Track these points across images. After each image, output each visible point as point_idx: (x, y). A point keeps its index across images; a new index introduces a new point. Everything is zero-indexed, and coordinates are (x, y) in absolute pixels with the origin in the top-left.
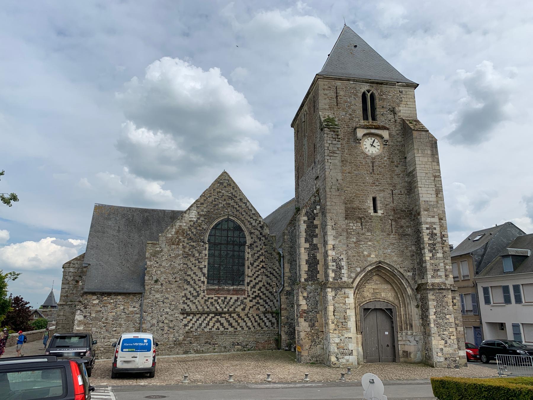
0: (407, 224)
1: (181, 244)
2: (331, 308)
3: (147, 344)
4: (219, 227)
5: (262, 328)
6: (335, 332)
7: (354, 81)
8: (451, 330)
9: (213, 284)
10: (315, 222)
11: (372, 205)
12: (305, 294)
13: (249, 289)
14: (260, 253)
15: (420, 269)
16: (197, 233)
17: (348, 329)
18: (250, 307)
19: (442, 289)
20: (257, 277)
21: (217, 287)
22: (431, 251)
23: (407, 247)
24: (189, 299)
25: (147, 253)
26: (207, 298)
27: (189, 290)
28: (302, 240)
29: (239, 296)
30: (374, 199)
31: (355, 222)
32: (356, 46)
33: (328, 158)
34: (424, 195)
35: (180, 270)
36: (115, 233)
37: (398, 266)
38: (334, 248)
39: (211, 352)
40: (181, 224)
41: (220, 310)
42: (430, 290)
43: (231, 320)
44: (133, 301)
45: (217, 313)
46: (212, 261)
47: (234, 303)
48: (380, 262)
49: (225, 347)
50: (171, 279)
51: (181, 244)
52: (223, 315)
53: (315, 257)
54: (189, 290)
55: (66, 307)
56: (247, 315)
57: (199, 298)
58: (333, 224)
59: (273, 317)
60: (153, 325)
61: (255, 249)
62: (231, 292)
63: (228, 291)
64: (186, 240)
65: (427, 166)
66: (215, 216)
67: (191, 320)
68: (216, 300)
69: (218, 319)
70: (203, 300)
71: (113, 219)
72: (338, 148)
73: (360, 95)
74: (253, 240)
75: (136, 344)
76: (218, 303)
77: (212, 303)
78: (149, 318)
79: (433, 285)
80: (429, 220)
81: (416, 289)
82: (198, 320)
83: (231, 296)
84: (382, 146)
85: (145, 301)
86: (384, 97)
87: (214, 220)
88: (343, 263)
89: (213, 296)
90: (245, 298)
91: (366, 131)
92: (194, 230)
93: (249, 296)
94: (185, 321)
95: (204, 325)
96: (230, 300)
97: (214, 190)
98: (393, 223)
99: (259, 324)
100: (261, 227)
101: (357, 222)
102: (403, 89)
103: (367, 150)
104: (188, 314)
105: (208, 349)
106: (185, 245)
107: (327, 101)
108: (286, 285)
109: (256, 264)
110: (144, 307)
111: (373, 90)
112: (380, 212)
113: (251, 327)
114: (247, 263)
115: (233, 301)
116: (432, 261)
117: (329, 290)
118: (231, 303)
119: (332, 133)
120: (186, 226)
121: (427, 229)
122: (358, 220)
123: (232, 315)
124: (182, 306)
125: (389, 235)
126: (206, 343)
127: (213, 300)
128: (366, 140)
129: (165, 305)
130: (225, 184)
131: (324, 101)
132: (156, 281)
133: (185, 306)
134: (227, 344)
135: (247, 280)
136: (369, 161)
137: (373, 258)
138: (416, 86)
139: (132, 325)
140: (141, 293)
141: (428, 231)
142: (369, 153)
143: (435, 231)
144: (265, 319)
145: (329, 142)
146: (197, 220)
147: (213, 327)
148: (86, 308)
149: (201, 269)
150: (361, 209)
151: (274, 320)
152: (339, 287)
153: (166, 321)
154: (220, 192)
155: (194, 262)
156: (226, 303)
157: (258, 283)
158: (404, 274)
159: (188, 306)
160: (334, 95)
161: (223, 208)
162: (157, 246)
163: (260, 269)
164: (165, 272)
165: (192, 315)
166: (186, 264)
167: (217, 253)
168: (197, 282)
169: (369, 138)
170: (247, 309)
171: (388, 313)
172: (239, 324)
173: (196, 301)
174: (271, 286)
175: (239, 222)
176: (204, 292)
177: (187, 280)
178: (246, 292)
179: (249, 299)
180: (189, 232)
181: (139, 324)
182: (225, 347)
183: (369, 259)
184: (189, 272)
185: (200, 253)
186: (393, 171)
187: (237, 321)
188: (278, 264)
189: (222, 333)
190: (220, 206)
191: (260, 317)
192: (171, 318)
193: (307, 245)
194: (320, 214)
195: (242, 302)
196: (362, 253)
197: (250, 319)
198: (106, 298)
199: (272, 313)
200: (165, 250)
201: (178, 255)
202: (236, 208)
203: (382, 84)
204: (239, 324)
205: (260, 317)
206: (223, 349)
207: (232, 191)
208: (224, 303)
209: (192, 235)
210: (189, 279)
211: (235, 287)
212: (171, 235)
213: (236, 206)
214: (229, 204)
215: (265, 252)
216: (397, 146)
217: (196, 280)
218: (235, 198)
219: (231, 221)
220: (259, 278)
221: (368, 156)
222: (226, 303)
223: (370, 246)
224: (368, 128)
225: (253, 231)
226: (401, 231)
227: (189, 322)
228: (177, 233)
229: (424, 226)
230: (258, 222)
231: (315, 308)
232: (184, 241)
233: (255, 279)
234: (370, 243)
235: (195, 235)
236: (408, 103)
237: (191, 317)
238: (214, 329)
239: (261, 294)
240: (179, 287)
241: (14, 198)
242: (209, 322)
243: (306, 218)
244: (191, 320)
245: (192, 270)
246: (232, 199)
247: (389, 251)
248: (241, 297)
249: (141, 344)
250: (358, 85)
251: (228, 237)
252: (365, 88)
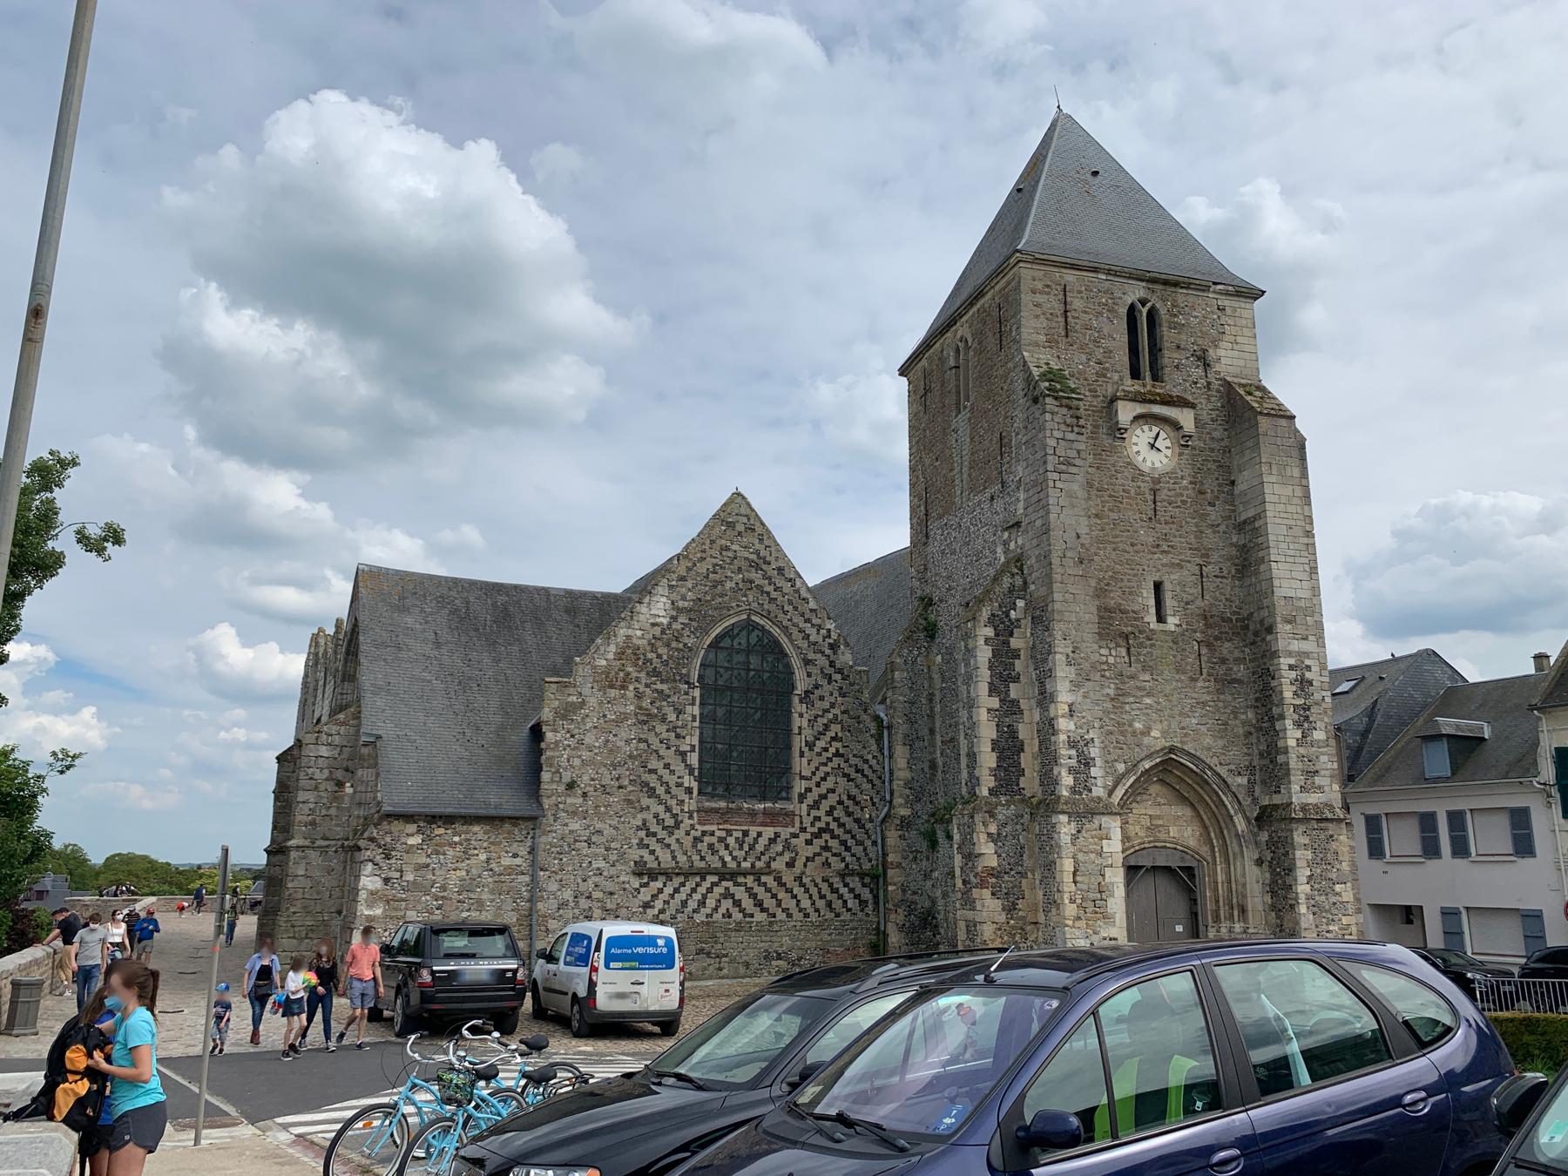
0: (1237, 654)
1: (631, 688)
2: (1068, 865)
3: (665, 950)
4: (727, 642)
5: (838, 915)
6: (1077, 924)
7: (1108, 272)
8: (1345, 920)
9: (713, 796)
10: (1015, 643)
11: (1152, 602)
12: (993, 829)
13: (804, 813)
14: (830, 716)
15: (1269, 766)
16: (671, 657)
17: (1107, 918)
18: (808, 859)
19: (1327, 820)
20: (824, 779)
21: (723, 804)
22: (1298, 725)
23: (1235, 713)
24: (654, 835)
25: (546, 710)
26: (698, 834)
27: (653, 810)
28: (983, 688)
29: (778, 829)
30: (1158, 586)
31: (1112, 645)
32: (1095, 173)
33: (1056, 476)
34: (1285, 583)
35: (630, 757)
36: (428, 649)
37: (1215, 760)
38: (1071, 713)
39: (710, 978)
40: (630, 632)
41: (732, 865)
42: (1299, 820)
43: (760, 891)
44: (511, 840)
45: (725, 875)
46: (708, 732)
47: (767, 847)
48: (1172, 750)
49: (747, 965)
50: (606, 781)
51: (631, 688)
52: (741, 880)
53: (1013, 733)
54: (653, 810)
55: (312, 854)
56: (799, 879)
57: (680, 834)
58: (1069, 650)
59: (864, 885)
60: (563, 905)
61: (818, 704)
62: (760, 818)
63: (752, 813)
64: (643, 675)
65: (1291, 509)
66: (715, 613)
67: (661, 891)
68: (721, 840)
69: (727, 889)
70: (690, 838)
71: (417, 610)
72: (1078, 452)
73: (1123, 311)
74: (812, 681)
75: (640, 950)
76: (727, 847)
77: (711, 846)
78: (553, 887)
79: (1304, 808)
80: (1296, 646)
81: (1257, 819)
82: (676, 891)
83: (760, 829)
84: (1177, 450)
85: (543, 839)
86: (1181, 319)
87: (714, 622)
88: (1094, 752)
89: (714, 828)
90: (795, 836)
91: (1140, 409)
92: (663, 651)
93: (803, 830)
94: (645, 895)
95: (692, 904)
96: (756, 840)
97: (713, 542)
98: (1204, 651)
99: (829, 904)
100: (831, 646)
101: (1118, 645)
102: (1226, 303)
103: (1140, 458)
104: (653, 875)
105: (705, 969)
106: (642, 688)
107: (1042, 323)
108: (898, 801)
109: (820, 744)
110: (541, 856)
111: (1154, 300)
112: (1172, 622)
113: (810, 910)
114: (798, 743)
115: (763, 841)
116: (1302, 750)
117: (1064, 818)
118: (759, 848)
119: (1064, 411)
120: (642, 637)
121: (1291, 667)
122: (1122, 642)
123: (764, 879)
124: (635, 854)
125: (1195, 680)
126: (700, 952)
127: (714, 840)
128: (1138, 432)
129: (594, 849)
130: (740, 528)
131: (1033, 323)
132: (571, 786)
133: (645, 853)
134: (751, 955)
135: (799, 786)
136: (1145, 487)
137: (1156, 739)
138: (1255, 294)
139: (509, 905)
140: (533, 819)
141: (1293, 674)
142: (1146, 467)
143: (1308, 675)
144: (843, 890)
145: (1057, 434)
146: (670, 624)
147: (716, 909)
148: (388, 857)
149: (683, 754)
150: (1126, 612)
151: (866, 894)
152: (1086, 813)
153: (596, 895)
154: (727, 549)
155: (665, 735)
156: (746, 847)
157: (823, 797)
158: (1229, 780)
159: (652, 852)
162: (572, 690)
163: (830, 760)
164: (592, 762)
165: (662, 879)
166: (646, 741)
167: (720, 712)
168: (674, 790)
169: (1146, 428)
170: (799, 864)
171: (1184, 878)
172: (779, 904)
173: (671, 841)
174: (857, 803)
175: (776, 631)
176: (691, 817)
177: (647, 784)
178: (797, 819)
179: (804, 837)
180: (650, 656)
181: (530, 901)
182: (747, 965)
183: (1146, 740)
184: (654, 763)
185: (679, 712)
186: (1204, 516)
187: (774, 896)
188: (874, 747)
189: (739, 927)
190: (729, 585)
191: (831, 885)
192: (610, 886)
193: (995, 703)
194: (1027, 623)
195: (787, 846)
196: (1131, 725)
197: (807, 891)
198: (442, 831)
199: (862, 875)
200: (592, 701)
201: (626, 717)
202: (768, 593)
203: (1176, 284)
204: (779, 904)
205: (831, 885)
206: (742, 970)
207: (758, 546)
208: (741, 848)
209: (656, 665)
210: (652, 780)
211: (769, 805)
212: (604, 663)
213: (767, 589)
214: (751, 582)
215: (843, 712)
216: (1212, 450)
217: (672, 784)
218: (764, 567)
219: (756, 626)
220: (829, 783)
221: (1142, 473)
222: (746, 847)
223: (1150, 707)
224: (1144, 401)
225: (811, 656)
226: (1221, 670)
227: (655, 897)
228: (620, 655)
229: (1285, 662)
230: (823, 632)
231: (1017, 864)
232: (637, 680)
233: (818, 785)
234: (1148, 701)
235: (666, 663)
236: (1239, 339)
237: (659, 884)
238: (718, 916)
239: (833, 825)
240: (629, 802)
241: (115, 536)
242: (704, 897)
243: (990, 632)
244: (661, 891)
245: (660, 757)
246: (758, 568)
247: (1194, 721)
248: (785, 832)
249: (651, 950)
250: (1118, 285)
251: (749, 670)
252: (1135, 292)
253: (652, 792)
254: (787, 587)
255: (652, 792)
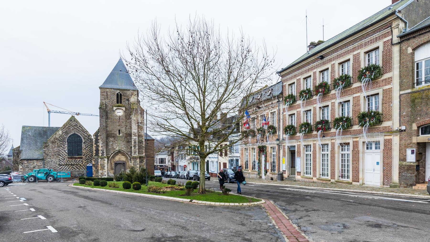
63: (76, 158)
73: (116, 94)
80: (135, 138)
88: (105, 151)
91: (116, 108)
94: (60, 167)
104: (61, 165)
112: (121, 135)
135: (83, 154)
137: (117, 149)
160: (106, 94)
161: (73, 129)
175: (79, 134)
184: (60, 152)
185: (64, 146)
189: (74, 171)
229: (132, 140)
248: (81, 160)
252: (118, 91)
253: (60, 156)
254: (81, 128)
255: (60, 156)
